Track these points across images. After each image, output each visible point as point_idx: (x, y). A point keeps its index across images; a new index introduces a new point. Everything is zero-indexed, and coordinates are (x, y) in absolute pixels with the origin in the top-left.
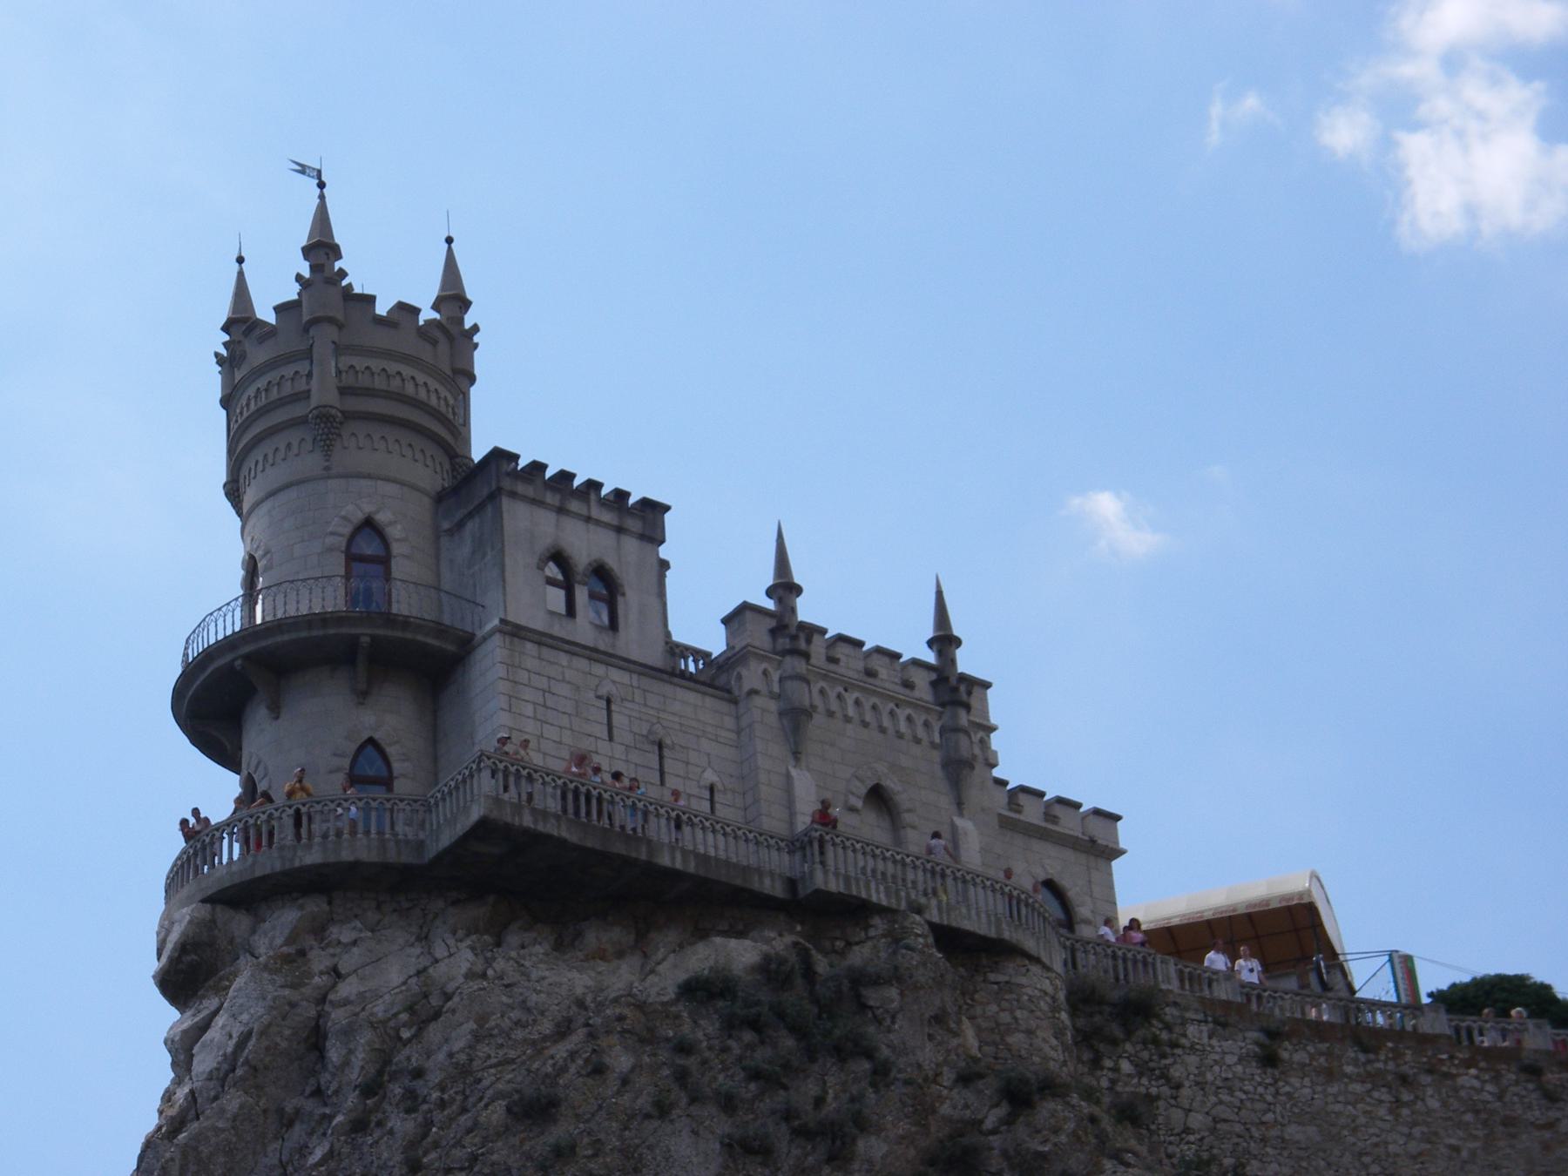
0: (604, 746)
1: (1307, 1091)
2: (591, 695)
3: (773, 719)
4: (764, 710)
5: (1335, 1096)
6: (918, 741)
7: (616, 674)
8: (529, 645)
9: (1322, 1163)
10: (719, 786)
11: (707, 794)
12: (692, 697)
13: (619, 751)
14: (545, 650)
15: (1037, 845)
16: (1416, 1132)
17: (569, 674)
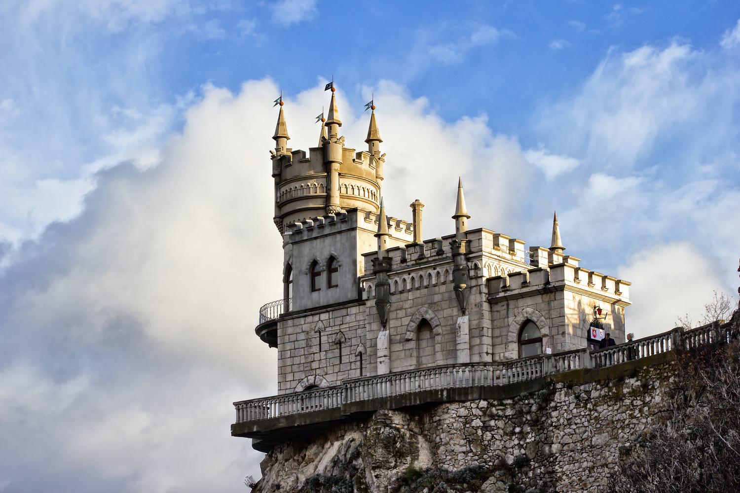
0: (317, 357)
1: (605, 411)
2: (313, 333)
3: (374, 311)
4: (370, 307)
5: (617, 410)
6: (444, 283)
7: (324, 316)
8: (290, 322)
9: (608, 454)
10: (363, 352)
11: (359, 358)
12: (354, 310)
13: (323, 354)
14: (295, 320)
15: (521, 302)
16: (649, 419)
17: (306, 327)
